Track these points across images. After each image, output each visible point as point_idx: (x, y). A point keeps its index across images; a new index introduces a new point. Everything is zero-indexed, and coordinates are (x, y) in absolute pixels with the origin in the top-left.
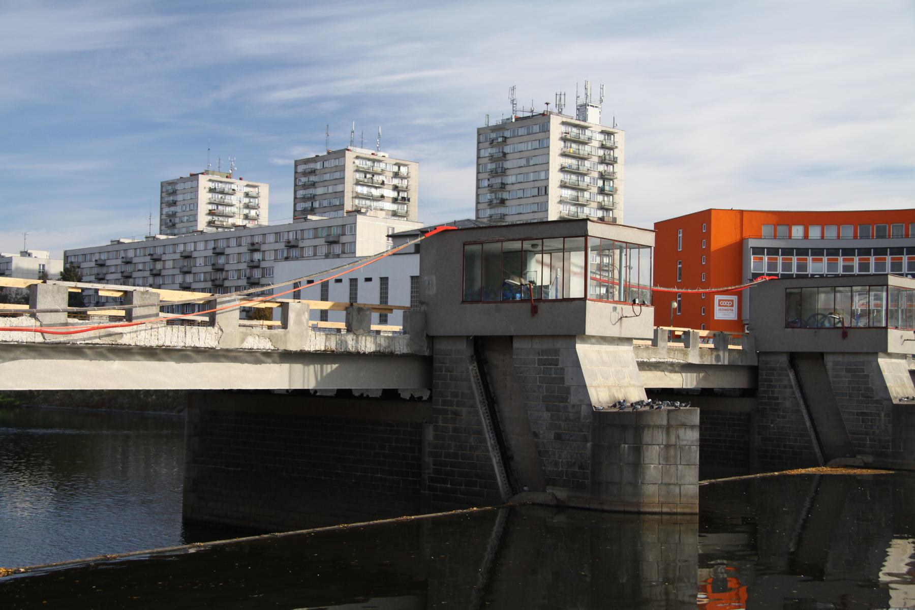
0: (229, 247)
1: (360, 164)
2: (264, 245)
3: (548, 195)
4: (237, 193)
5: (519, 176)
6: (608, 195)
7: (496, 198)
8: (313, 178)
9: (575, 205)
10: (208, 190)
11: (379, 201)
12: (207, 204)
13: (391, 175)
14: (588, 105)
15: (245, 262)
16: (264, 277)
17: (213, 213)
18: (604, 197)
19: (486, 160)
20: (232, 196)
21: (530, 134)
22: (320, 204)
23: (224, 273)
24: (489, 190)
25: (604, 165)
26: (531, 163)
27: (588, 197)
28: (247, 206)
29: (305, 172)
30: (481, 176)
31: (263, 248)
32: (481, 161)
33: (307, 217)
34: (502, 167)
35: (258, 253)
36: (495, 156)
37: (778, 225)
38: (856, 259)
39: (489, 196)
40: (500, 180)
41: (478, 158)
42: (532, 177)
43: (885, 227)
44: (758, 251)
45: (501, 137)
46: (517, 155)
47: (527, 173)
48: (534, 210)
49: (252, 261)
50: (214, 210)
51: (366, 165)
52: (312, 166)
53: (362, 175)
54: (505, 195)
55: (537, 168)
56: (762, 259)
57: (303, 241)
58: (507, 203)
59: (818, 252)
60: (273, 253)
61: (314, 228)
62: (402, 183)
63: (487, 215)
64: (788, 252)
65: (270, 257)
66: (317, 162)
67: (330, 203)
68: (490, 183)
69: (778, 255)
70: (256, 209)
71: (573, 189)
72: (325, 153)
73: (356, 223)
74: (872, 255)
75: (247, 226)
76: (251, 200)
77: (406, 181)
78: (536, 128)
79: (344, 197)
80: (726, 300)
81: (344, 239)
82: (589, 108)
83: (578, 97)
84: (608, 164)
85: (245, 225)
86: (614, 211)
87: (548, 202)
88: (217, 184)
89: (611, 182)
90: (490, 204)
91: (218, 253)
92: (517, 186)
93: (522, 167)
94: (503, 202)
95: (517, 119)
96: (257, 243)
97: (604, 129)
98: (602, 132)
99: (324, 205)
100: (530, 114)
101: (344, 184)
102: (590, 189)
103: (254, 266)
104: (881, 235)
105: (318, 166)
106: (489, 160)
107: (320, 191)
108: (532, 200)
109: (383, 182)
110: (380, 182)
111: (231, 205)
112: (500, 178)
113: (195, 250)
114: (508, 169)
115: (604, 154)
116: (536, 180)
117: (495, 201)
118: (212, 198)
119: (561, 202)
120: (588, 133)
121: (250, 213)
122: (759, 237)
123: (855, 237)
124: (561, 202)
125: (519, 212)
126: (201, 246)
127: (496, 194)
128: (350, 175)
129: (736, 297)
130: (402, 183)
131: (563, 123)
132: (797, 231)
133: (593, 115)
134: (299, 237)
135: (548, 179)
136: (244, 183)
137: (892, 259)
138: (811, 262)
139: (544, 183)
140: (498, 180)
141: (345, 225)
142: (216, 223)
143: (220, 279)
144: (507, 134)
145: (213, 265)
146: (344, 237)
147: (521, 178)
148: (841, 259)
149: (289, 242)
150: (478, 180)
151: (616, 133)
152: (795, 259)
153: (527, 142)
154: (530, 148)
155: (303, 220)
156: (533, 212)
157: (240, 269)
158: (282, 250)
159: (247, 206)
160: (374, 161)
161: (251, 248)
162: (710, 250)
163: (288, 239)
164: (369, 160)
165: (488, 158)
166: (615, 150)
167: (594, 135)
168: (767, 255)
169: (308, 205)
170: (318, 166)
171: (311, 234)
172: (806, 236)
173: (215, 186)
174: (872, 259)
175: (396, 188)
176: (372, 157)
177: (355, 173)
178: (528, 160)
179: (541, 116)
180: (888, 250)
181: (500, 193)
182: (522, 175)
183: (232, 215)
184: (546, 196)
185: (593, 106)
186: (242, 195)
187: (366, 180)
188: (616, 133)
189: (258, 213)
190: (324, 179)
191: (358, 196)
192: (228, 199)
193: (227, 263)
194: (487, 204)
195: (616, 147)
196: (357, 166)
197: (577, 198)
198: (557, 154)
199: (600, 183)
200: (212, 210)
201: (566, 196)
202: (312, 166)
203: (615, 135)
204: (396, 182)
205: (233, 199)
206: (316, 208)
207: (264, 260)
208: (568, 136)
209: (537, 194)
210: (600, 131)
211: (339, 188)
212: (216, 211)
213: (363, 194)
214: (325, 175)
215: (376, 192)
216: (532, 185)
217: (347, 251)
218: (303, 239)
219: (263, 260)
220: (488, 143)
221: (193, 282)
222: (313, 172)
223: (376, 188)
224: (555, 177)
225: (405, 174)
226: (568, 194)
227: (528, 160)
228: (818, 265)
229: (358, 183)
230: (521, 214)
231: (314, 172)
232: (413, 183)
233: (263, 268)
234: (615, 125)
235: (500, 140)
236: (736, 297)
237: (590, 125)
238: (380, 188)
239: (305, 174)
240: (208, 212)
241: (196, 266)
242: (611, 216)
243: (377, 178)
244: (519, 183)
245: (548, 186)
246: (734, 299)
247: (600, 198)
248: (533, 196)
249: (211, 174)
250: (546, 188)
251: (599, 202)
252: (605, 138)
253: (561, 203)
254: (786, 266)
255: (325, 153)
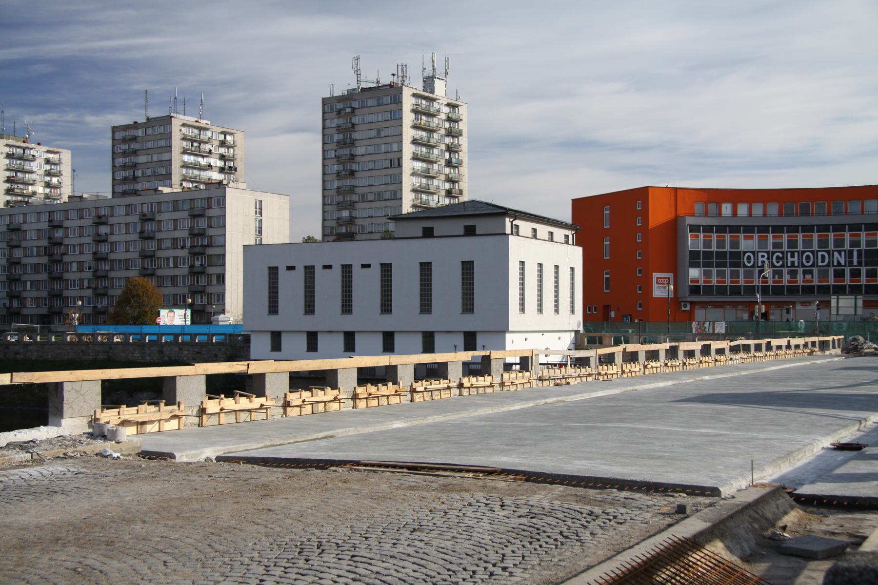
0: (68, 219)
1: (186, 132)
2: (112, 218)
3: (401, 167)
4: (37, 159)
5: (369, 148)
6: (454, 167)
7: (344, 170)
8: (134, 146)
9: (426, 177)
10: (5, 155)
11: (207, 170)
12: (4, 170)
13: (217, 143)
14: (435, 77)
15: (89, 236)
16: (113, 252)
17: (12, 180)
18: (450, 169)
19: (334, 131)
20: (32, 163)
21: (380, 105)
22: (143, 173)
23: (63, 247)
24: (337, 161)
25: (450, 137)
26: (383, 134)
27: (437, 169)
28: (48, 174)
29: (125, 138)
30: (327, 147)
31: (112, 220)
32: (327, 131)
33: (158, 189)
34: (351, 138)
35: (105, 226)
36: (344, 126)
37: (709, 202)
38: (785, 236)
39: (336, 168)
40: (348, 150)
41: (324, 128)
42: (383, 148)
43: (809, 204)
44: (694, 229)
45: (348, 107)
46: (368, 126)
47: (378, 145)
48: (387, 182)
49: (99, 235)
50: (13, 177)
51: (192, 132)
52: (132, 132)
53: (189, 144)
54: (354, 167)
55: (389, 140)
56: (697, 236)
57: (161, 214)
58: (357, 175)
59: (749, 230)
60: (123, 226)
61: (174, 201)
62: (228, 152)
63: (335, 187)
64: (721, 229)
65: (120, 231)
66: (138, 129)
67: (155, 172)
68: (337, 154)
69: (700, 232)
70: (58, 176)
71: (423, 161)
72: (144, 120)
73: (225, 196)
74: (800, 232)
75: (84, 197)
76: (53, 167)
77: (232, 150)
78: (387, 100)
79: (171, 166)
80: (663, 278)
81: (210, 213)
82: (436, 80)
83: (424, 69)
84: (453, 137)
85: (82, 196)
86: (460, 183)
87: (401, 174)
88: (14, 149)
89: (457, 154)
90: (338, 175)
91: (54, 226)
92: (367, 158)
93: (372, 138)
94: (352, 173)
95: (363, 90)
96: (104, 216)
97: (450, 101)
98: (448, 105)
99: (148, 174)
100: (375, 85)
101: (171, 152)
102: (439, 161)
103: (100, 240)
104: (805, 212)
105: (140, 133)
106: (337, 130)
107: (142, 159)
108: (384, 172)
109: (211, 150)
110: (207, 150)
111: (31, 172)
112: (348, 150)
113: (25, 222)
114: (357, 140)
115: (450, 127)
116: (389, 152)
117: (343, 173)
118: (10, 164)
119: (413, 174)
120: (435, 105)
121: (51, 180)
122: (693, 215)
123: (780, 215)
124: (413, 174)
125: (370, 184)
126: (32, 218)
127: (344, 166)
128: (177, 144)
129: (672, 274)
130: (228, 152)
131: (414, 95)
132: (726, 209)
133: (440, 87)
134: (155, 209)
135: (401, 151)
136: (45, 148)
137: (819, 236)
138: (743, 239)
139: (397, 155)
140: (347, 151)
141: (212, 198)
142: (16, 190)
143: (57, 253)
144: (355, 104)
145: (50, 238)
146: (210, 210)
147: (371, 150)
148: (770, 236)
149: (144, 215)
150: (324, 151)
151: (461, 106)
152: (728, 237)
153: (377, 113)
154: (380, 119)
155: (153, 192)
156: (385, 184)
157: (82, 243)
158: (135, 224)
159: (48, 174)
160: (200, 129)
161: (97, 221)
162: (648, 227)
163: (142, 212)
164: (195, 127)
165: (335, 129)
166: (460, 123)
167: (441, 107)
168: (703, 232)
169: (129, 173)
170: (140, 133)
171: (171, 207)
172: (735, 213)
173: (13, 151)
174: (800, 236)
175: (222, 157)
176: (198, 125)
177: (182, 141)
178: (379, 132)
179: (389, 87)
180: (815, 227)
181: (349, 164)
182: (373, 147)
183: (33, 182)
184: (399, 168)
185: (439, 79)
186: (43, 162)
187: (193, 149)
188: (461, 106)
189: (60, 181)
190: (147, 147)
191: (185, 166)
192: (27, 166)
193: (66, 237)
194: (335, 175)
195: (461, 120)
196: (184, 134)
197: (428, 171)
198: (409, 126)
199: (447, 155)
200: (11, 177)
201: (418, 168)
202: (132, 132)
203: (460, 108)
204: (222, 150)
205: (34, 166)
206: (138, 177)
207: (112, 234)
208: (419, 109)
209: (389, 166)
210: (446, 103)
211: (165, 157)
212: (15, 178)
213: (191, 163)
214: (148, 143)
215: (203, 161)
216: (383, 156)
217: (214, 225)
218: (160, 212)
219: (111, 234)
220: (335, 113)
221: (24, 257)
222: (134, 139)
223: (203, 157)
224: (408, 149)
225: (232, 143)
226: (419, 165)
227: (379, 132)
228: (749, 242)
229: (185, 152)
230: (372, 185)
231: (136, 140)
232: (239, 152)
233: (112, 243)
234: (458, 98)
235: (349, 110)
236: (672, 274)
237: (438, 97)
238: (207, 156)
239: (124, 140)
240: (6, 179)
241: (26, 240)
242: (457, 188)
243: (206, 147)
244: (369, 154)
245: (402, 158)
246: (670, 276)
247: (447, 170)
248: (385, 168)
249: (6, 139)
250: (399, 160)
251: (446, 174)
252: (450, 110)
253: (413, 176)
254: (721, 243)
255: (144, 120)
